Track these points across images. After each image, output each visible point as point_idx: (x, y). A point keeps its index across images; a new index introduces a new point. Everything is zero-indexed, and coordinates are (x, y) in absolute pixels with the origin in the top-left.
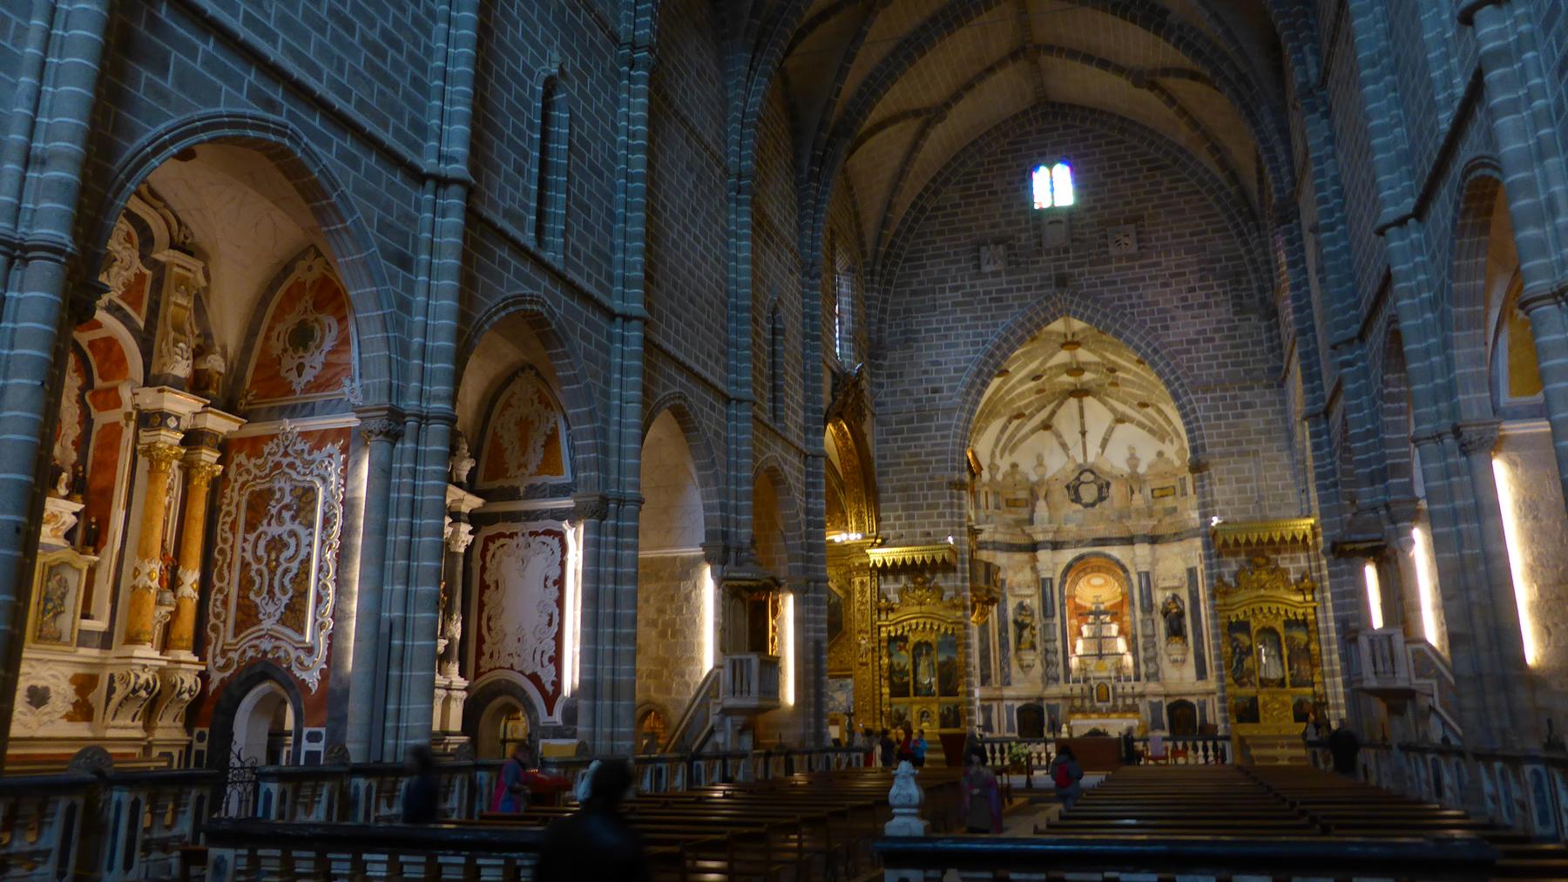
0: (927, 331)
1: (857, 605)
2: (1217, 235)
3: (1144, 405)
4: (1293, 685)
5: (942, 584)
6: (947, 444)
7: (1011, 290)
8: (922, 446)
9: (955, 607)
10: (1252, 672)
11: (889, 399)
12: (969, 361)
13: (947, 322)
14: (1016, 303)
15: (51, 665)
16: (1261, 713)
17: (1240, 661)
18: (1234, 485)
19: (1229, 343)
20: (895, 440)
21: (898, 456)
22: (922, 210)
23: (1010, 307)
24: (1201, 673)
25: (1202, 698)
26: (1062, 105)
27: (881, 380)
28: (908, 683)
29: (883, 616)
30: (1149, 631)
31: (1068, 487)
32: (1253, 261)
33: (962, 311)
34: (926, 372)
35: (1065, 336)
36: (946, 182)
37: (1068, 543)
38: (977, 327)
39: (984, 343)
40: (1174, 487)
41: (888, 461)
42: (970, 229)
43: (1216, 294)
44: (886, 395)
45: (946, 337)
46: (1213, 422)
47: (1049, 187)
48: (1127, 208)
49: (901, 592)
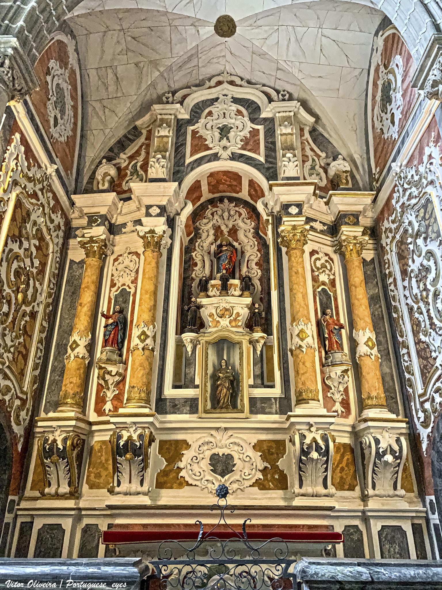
15: (230, 433)
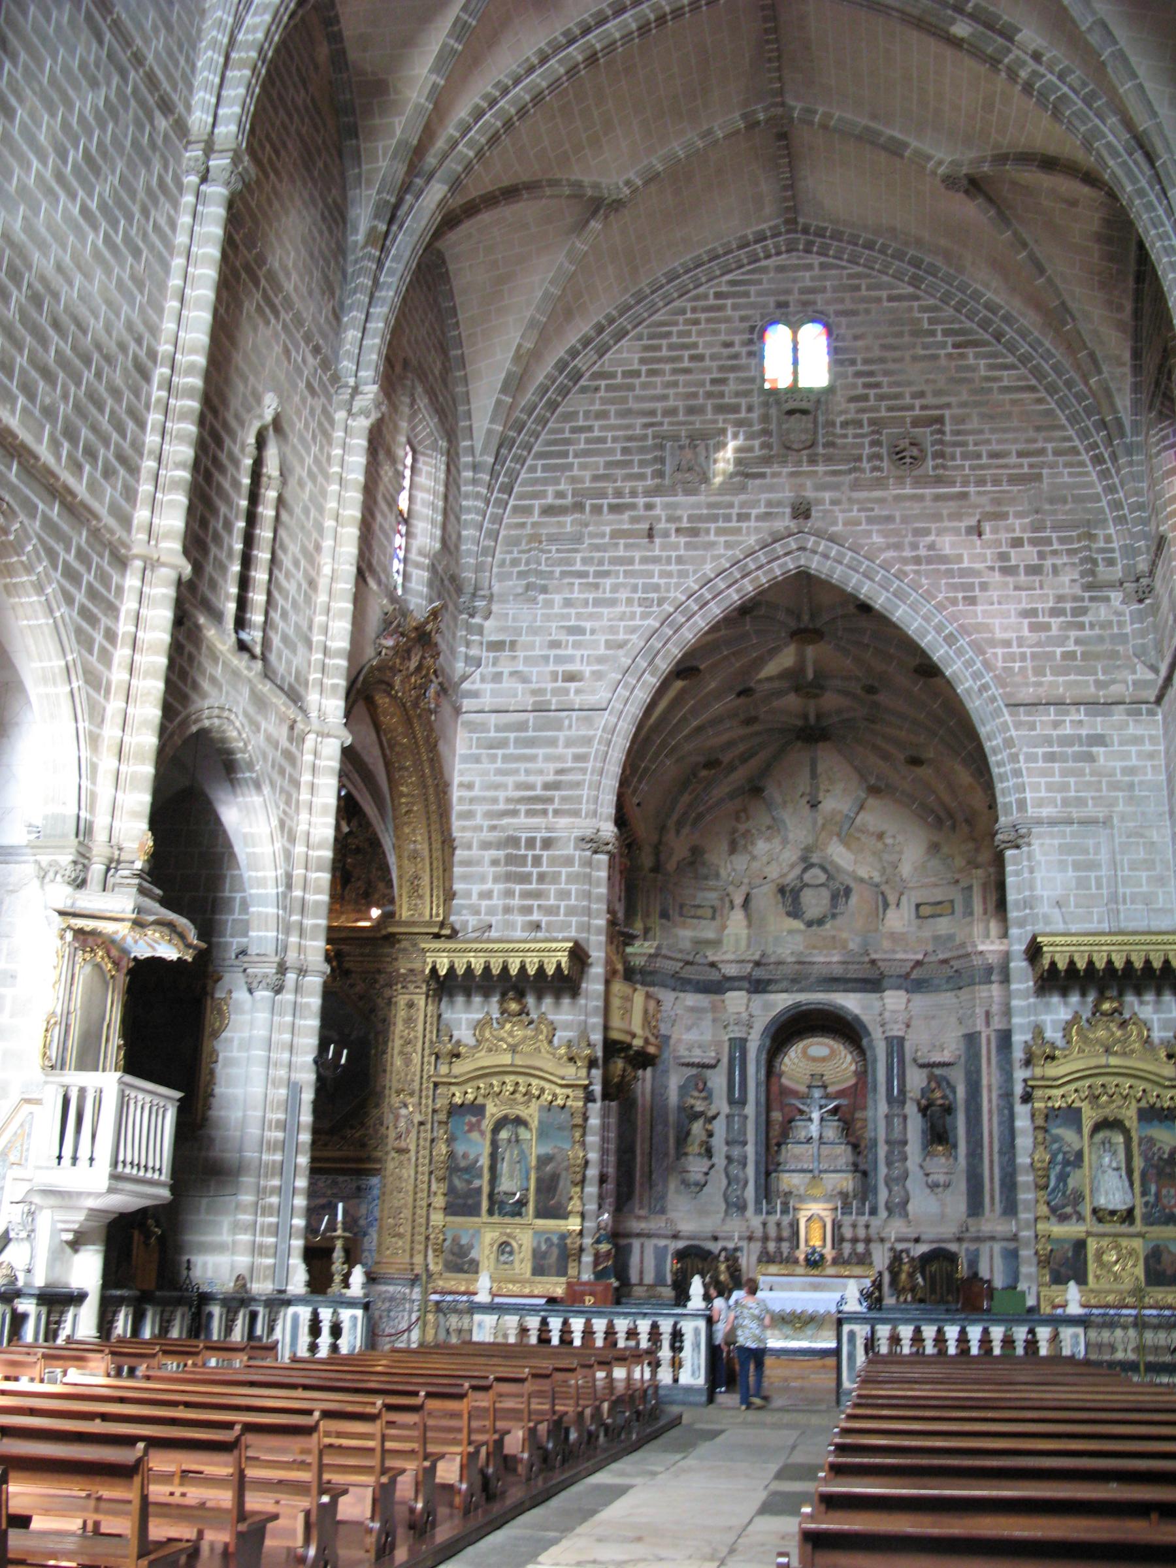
0: (564, 574)
1: (397, 1043)
2: (1061, 459)
3: (915, 761)
4: (1149, 1220)
5: (551, 1017)
6: (584, 771)
7: (714, 518)
8: (541, 772)
9: (571, 1059)
10: (1078, 1198)
11: (488, 687)
12: (633, 630)
13: (601, 562)
14: (722, 539)
16: (1092, 1266)
17: (1063, 1178)
18: (1070, 873)
19: (1073, 634)
20: (493, 759)
21: (497, 787)
22: (577, 376)
23: (711, 545)
24: (975, 1207)
25: (973, 1247)
26: (820, 233)
27: (474, 652)
28: (479, 1191)
29: (444, 1069)
30: (896, 1135)
31: (782, 890)
32: (1117, 505)
33: (626, 546)
34: (555, 644)
35: (799, 618)
36: (621, 334)
37: (776, 981)
38: (650, 575)
39: (661, 602)
40: (952, 902)
41: (476, 792)
42: (652, 413)
43: (1055, 553)
44: (483, 680)
45: (596, 586)
46: (1040, 764)
47: (791, 345)
48: (918, 403)
49: (480, 1026)
